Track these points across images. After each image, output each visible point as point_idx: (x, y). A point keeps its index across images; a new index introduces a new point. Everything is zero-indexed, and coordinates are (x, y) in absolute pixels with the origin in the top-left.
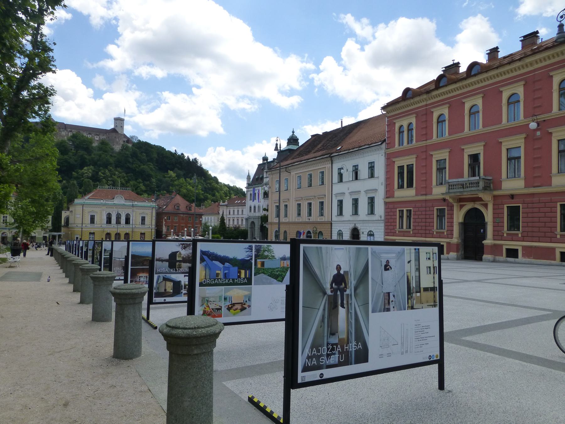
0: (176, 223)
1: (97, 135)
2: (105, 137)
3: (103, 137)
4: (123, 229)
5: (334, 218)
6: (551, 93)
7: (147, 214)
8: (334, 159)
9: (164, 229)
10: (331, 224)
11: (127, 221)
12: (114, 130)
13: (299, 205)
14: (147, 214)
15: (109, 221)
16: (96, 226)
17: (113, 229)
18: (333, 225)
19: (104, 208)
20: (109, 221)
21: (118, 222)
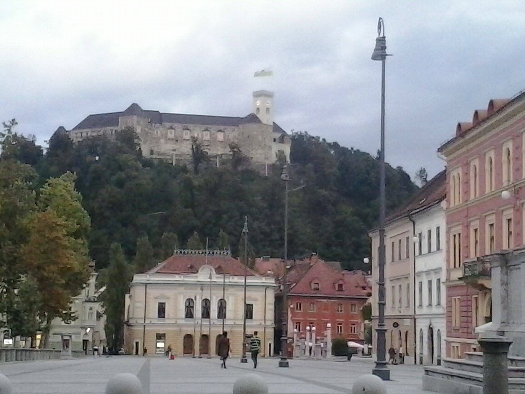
0: (313, 315)
1: (220, 131)
2: (235, 134)
3: (232, 134)
4: (214, 328)
5: (417, 312)
6: (495, 163)
7: (256, 300)
8: (414, 217)
9: (291, 329)
10: (415, 319)
11: (222, 314)
12: (253, 118)
13: (393, 287)
14: (256, 300)
15: (189, 315)
16: (167, 321)
17: (197, 327)
18: (417, 320)
19: (182, 289)
20: (189, 315)
21: (206, 314)
